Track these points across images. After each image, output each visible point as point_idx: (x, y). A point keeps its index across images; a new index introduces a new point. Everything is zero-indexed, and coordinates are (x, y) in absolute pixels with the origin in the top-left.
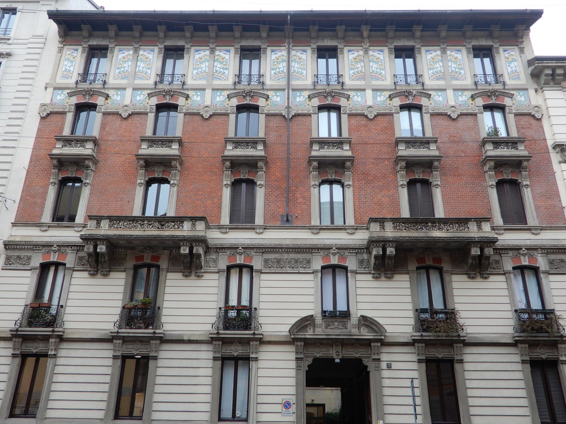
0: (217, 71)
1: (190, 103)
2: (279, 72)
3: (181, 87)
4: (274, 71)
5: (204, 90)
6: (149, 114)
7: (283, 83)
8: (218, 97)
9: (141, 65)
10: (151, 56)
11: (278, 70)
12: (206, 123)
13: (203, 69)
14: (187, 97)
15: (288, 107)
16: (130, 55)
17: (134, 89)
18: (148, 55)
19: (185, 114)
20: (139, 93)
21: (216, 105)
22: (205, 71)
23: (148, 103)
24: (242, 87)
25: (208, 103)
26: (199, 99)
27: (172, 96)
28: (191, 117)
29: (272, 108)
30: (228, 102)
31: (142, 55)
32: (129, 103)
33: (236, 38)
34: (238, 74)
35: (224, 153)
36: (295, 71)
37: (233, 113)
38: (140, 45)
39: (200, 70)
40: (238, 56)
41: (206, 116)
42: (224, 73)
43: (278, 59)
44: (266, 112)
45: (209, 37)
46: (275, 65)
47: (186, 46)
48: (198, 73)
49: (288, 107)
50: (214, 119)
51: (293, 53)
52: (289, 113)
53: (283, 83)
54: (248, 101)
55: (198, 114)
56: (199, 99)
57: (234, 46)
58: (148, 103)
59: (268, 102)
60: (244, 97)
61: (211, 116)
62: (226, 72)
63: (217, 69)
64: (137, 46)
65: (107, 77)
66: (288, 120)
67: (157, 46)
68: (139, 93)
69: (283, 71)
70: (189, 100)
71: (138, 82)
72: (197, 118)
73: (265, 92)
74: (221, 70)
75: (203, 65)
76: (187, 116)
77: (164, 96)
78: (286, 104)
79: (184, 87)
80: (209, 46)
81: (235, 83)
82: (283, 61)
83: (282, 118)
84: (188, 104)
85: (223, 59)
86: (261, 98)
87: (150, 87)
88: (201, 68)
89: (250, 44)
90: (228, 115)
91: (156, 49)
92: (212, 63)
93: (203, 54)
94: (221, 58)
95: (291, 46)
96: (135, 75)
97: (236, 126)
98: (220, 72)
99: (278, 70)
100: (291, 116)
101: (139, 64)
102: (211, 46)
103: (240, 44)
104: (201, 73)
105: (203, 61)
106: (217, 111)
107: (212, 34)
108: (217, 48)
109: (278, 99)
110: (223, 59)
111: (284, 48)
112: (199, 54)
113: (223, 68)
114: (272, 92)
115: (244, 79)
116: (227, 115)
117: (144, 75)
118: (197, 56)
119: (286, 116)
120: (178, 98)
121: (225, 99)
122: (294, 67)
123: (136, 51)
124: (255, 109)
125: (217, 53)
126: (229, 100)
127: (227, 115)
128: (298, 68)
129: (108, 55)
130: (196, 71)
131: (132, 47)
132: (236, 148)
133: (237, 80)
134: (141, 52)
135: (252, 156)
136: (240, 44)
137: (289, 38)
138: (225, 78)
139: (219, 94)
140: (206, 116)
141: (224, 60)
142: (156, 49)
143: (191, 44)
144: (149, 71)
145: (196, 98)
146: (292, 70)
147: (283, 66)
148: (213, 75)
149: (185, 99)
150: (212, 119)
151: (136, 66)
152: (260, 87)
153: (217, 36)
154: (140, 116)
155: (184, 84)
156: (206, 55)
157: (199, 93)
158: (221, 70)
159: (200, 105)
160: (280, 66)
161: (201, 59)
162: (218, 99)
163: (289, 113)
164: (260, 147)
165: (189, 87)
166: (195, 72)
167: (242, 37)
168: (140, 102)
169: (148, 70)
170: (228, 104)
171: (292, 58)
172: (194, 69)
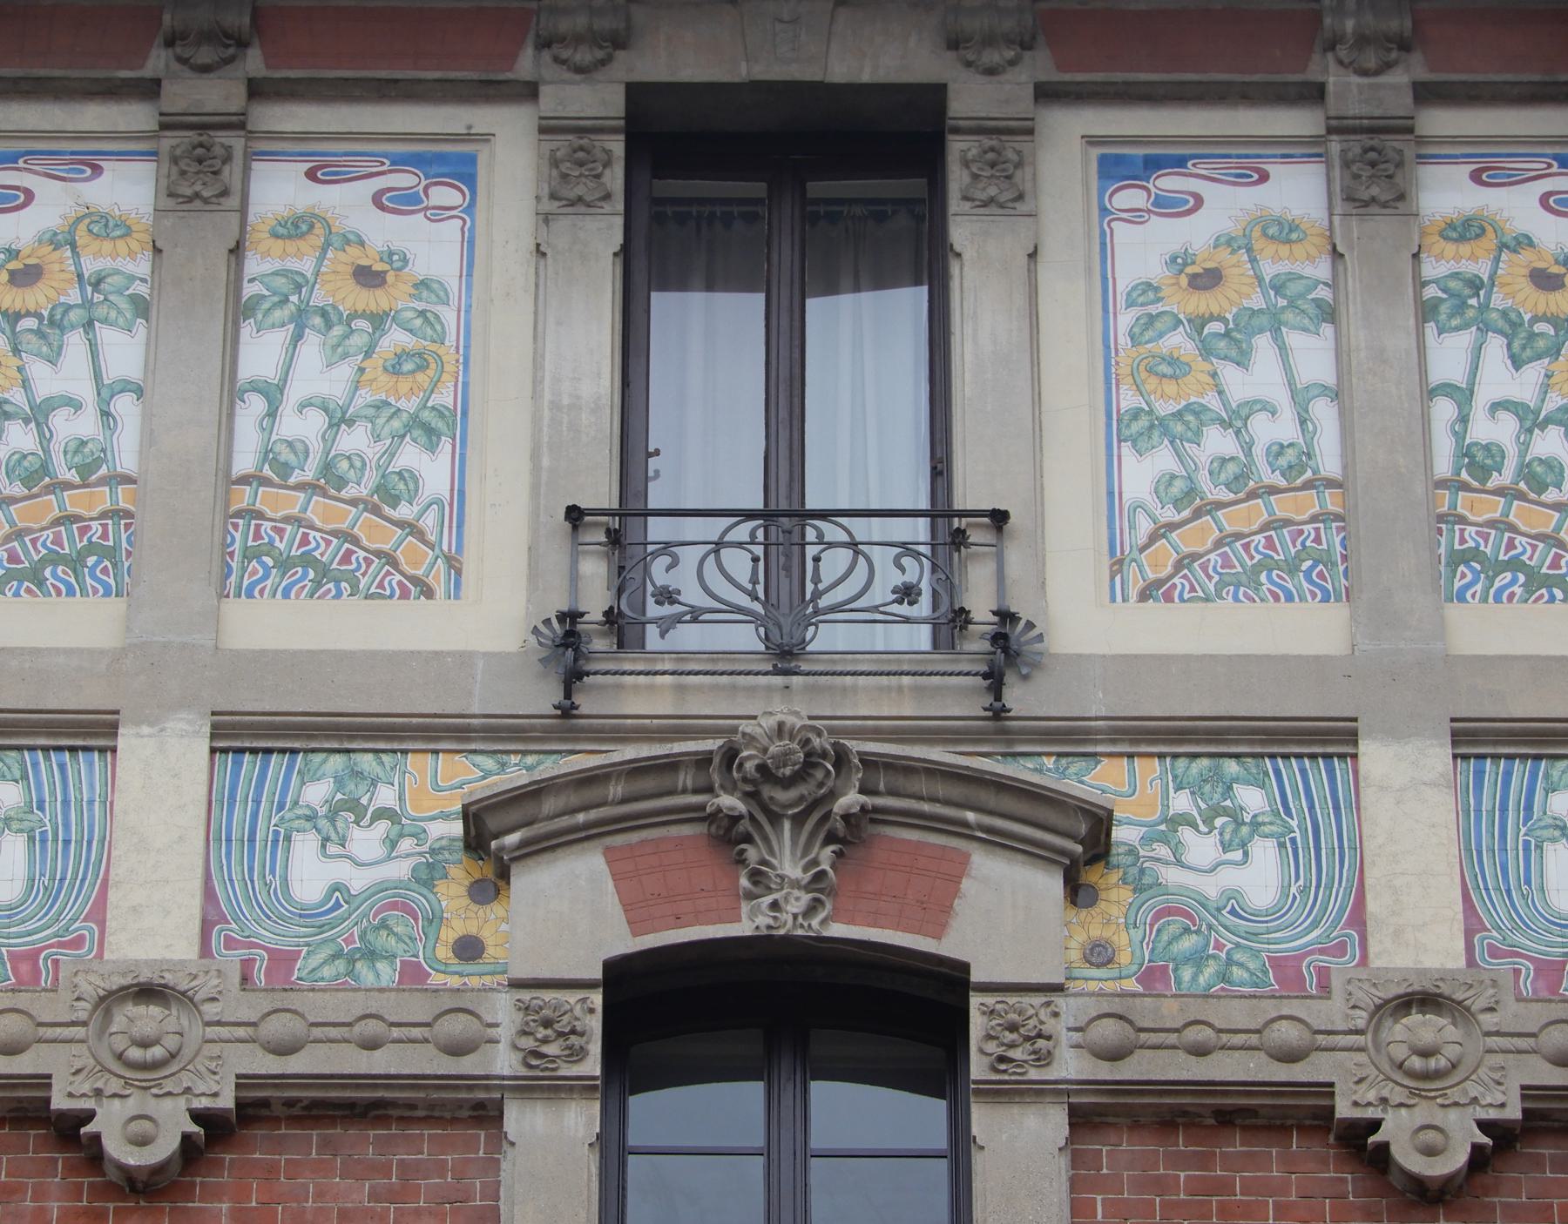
0: (1478, 462)
1: (1131, 948)
3: (961, 701)
5: (1332, 739)
6: (520, 1119)
9: (302, 380)
10: (430, 246)
13: (1264, 431)
14: (1083, 850)
16: (107, 226)
17: (235, 736)
18: (384, 232)
19: (1084, 1121)
20: (316, 793)
22: (1297, 466)
23: (469, 949)
26: (1260, 877)
27: (850, 836)
28: (1176, 1167)
31: (296, 227)
32: (184, 949)
34: (600, 492)
38: (257, 90)
39: (1218, 442)
47: (970, 98)
54: (780, 900)
55: (1293, 1116)
56: (1260, 877)
58: (469, 949)
63: (1482, 429)
64: (217, 94)
65: (1015, 557)
67: (529, 92)
68: (316, 793)
70: (1116, 896)
71: (281, 628)
73: (1039, 770)
75: (1259, 378)
76: (1118, 1153)
77: (729, 836)
79: (1020, 698)
80: (1314, 94)
81: (566, 643)
84: (1100, 954)
87: (479, 701)
88: (1236, 420)
91: (510, 145)
92: (1400, 342)
93: (1224, 207)
94: (1514, 268)
96: (240, 532)
101: (260, 353)
102: (1349, 91)
104: (1245, 487)
108: (1440, 121)
112: (1167, 206)
114: (1149, 771)
115: (703, 573)
117: (363, 524)
118: (1144, 249)
120: (953, 874)
123: (202, 167)
124: (907, 1019)
128: (1531, 420)
129: (962, 232)
130: (1163, 460)
131: (136, 116)
133: (595, 602)
134: (277, 189)
142: (510, 145)
143: (1041, 65)
144: (433, 471)
145: (1216, 865)
149: (1052, 884)
151: (232, 391)
154: (367, 1143)
155: (1008, 647)
156: (1284, 231)
157: (1252, 799)
159: (1286, 969)
161: (1208, 280)
165: (1096, 704)
166: (1141, 474)
168: (348, 932)
169: (410, 456)
172: (1125, 430)
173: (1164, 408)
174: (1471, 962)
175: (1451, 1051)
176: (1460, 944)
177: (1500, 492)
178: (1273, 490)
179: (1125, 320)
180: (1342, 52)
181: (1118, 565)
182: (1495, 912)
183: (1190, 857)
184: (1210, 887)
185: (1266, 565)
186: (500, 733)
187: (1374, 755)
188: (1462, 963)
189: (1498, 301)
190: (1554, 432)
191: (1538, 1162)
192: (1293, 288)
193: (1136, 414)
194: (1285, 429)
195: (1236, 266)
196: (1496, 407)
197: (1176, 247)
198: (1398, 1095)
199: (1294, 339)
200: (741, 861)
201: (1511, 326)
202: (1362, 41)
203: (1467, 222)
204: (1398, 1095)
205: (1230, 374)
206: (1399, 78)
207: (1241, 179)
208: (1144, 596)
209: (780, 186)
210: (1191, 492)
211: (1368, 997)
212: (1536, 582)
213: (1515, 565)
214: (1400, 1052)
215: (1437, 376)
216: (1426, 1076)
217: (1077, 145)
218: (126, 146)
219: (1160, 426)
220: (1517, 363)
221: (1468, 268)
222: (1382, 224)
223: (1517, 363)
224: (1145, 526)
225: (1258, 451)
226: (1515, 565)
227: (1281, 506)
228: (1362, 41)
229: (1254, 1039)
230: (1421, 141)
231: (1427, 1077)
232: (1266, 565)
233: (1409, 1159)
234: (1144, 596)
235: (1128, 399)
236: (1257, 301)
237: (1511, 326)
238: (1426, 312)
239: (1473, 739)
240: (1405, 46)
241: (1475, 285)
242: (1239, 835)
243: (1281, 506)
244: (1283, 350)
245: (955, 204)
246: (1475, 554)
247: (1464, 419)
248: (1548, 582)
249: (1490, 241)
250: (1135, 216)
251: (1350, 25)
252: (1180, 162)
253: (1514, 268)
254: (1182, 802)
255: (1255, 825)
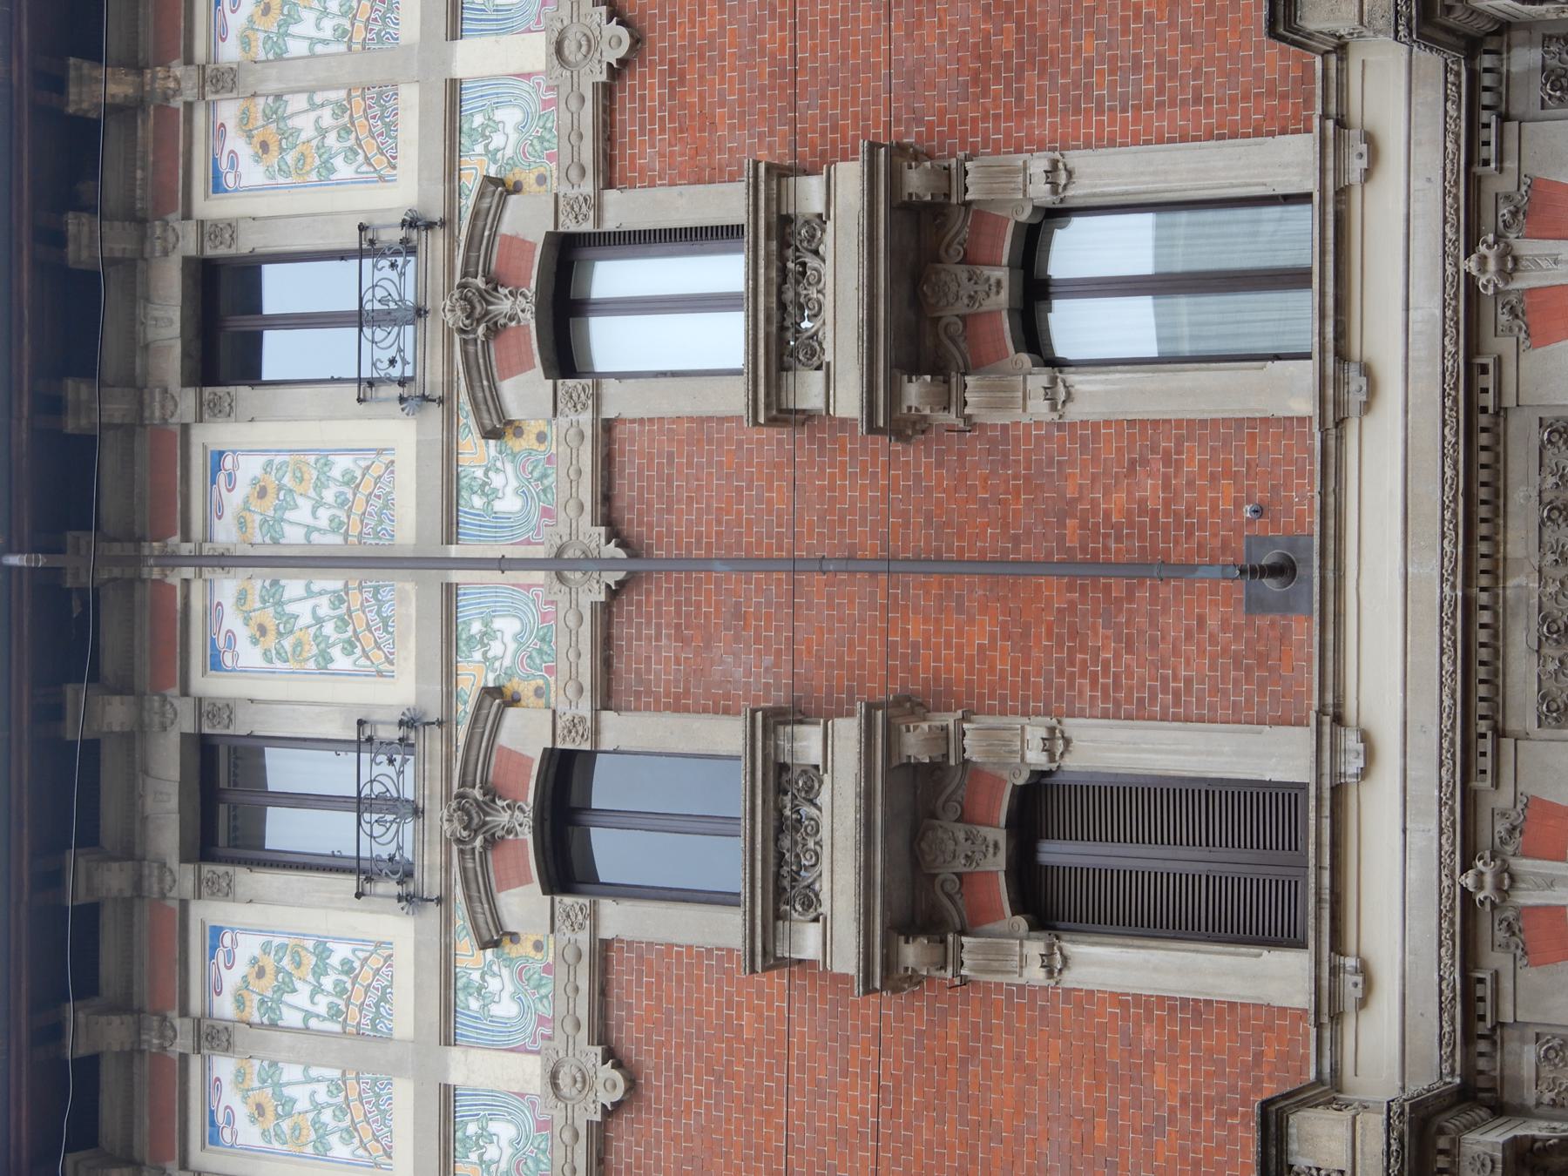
0: (335, 1013)
2: (343, 622)
4: (336, 652)
7: (407, 599)
8: (496, 1010)
11: (329, 629)
12: (656, 1083)
13: (322, 1097)
15: (558, 564)
21: (542, 1021)
22: (336, 1087)
24: (433, 857)
25: (528, 1072)
29: (563, 666)
30: (525, 948)
33: (138, 884)
34: (349, 883)
35: (844, 978)
36: (336, 526)
37: (594, 916)
39: (327, 1116)
40: (246, 879)
41: (609, 1085)
42: (347, 968)
43: (263, 630)
44: (585, 708)
45: (131, 1056)
46: (299, 644)
48: (350, 1132)
49: (558, 564)
50: (628, 1037)
51: (225, 534)
52: (590, 563)
53: (407, 599)
54: (518, 822)
56: (504, 1130)
57: (184, 904)
59: (526, 690)
60: (492, 842)
61: (611, 1055)
62: (340, 952)
63: (322, 1009)
66: (636, 565)
69: (338, 599)
72: (625, 1143)
73: (465, 710)
74: (328, 982)
78: (539, 576)
80: (184, 1058)
81: (411, 900)
82: (274, 596)
83: (627, 606)
85: (261, 973)
86: (504, 739)
88: (318, 1108)
89: (173, 803)
90: (606, 945)
92: (286, 1038)
93: (229, 1097)
94: (255, 985)
95: (186, 549)
97: (675, 905)
98: (341, 991)
99: (329, 629)
100: (613, 550)
102: (183, 1043)
103: (173, 861)
104: (344, 1109)
105: (278, 1096)
106: (583, 1013)
107: (112, 1034)
108: (195, 1006)
109: (508, 626)
110: (261, 973)
111: (197, 589)
112: (230, 1121)
113: (320, 970)
116: (603, 953)
119: (612, 578)
121: (509, 962)
122: (310, 530)
124: (565, 775)
125: (225, 1007)
126: (514, 937)
127: (603, 953)
128: (318, 504)
130: (334, 1140)
132: (810, 901)
133: (392, 887)
135: (867, 796)
136: (173, 861)
137: (138, 560)
138: (376, 961)
139: (474, 1004)
140: (609, 1085)
141: (269, 962)
146: (330, 541)
147: (307, 599)
148: (357, 1038)
150: (627, 1048)
152: (433, 742)
153: (125, 1006)
156: (240, 1075)
157: (472, 1129)
158: (328, 982)
159: (542, 1126)
160: (306, 619)
161: (260, 1108)
162: (506, 1008)
163: (590, 563)
164: (807, 744)
167: (132, 852)
170: (538, 946)
171: (258, 540)
173: (313, 1136)
174: (538, 1053)
175: (574, 1070)
176: (531, 1057)
177: (347, 1006)
178: (346, 1097)
179: (276, 1145)
180: (167, 1044)
181: (377, 1165)
182: (517, 1040)
183: (496, 1158)
184: (508, 1151)
185: (377, 1105)
186: (447, 922)
187: (454, 1079)
188: (538, 1058)
189: (269, 994)
190: (323, 980)
191: (619, 1039)
192: (264, 1075)
193: (315, 1148)
194: (322, 1088)
195: (255, 1097)
196: (312, 1002)
197: (247, 1120)
198: (591, 1096)
199: (284, 1079)
200: (502, 838)
201: (279, 990)
202: (162, 1036)
203: (237, 1001)
204: (591, 1096)
205: (299, 1107)
206: (177, 1022)
207: (219, 1089)
208: (390, 1157)
209: (225, 803)
210: (347, 1130)
211: (552, 1100)
212: (383, 998)
213: (377, 1006)
214: (574, 1092)
215: (300, 1024)
216: (584, 1082)
217: (205, 1154)
218: (206, 1069)
219: (320, 1138)
220: (294, 991)
221: (255, 1004)
222: (238, 1038)
223: (294, 991)
224: (361, 1152)
225: (331, 1101)
226: (377, 1006)
227: (353, 1096)
228: (162, 1036)
229: (570, 1149)
230: (203, 1014)
231: (584, 1081)
232: (377, 1105)
233: (618, 1094)
234: (390, 1157)
235: (309, 1150)
236: (269, 1091)
237: (279, 990)
238: (273, 1025)
239: (448, 1038)
240: (164, 1019)
241: (262, 1002)
242: (486, 1136)
243: (353, 1096)
244: (289, 1084)
245: (230, 731)
246: (373, 1021)
247: (318, 1016)
248: (384, 993)
249: (244, 992)
250: (234, 1134)
251: (156, 1041)
252: (212, 1112)
253: (255, 985)
254: (474, 1157)
255: (483, 1129)
